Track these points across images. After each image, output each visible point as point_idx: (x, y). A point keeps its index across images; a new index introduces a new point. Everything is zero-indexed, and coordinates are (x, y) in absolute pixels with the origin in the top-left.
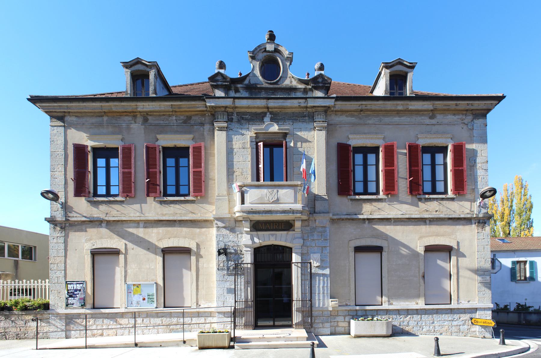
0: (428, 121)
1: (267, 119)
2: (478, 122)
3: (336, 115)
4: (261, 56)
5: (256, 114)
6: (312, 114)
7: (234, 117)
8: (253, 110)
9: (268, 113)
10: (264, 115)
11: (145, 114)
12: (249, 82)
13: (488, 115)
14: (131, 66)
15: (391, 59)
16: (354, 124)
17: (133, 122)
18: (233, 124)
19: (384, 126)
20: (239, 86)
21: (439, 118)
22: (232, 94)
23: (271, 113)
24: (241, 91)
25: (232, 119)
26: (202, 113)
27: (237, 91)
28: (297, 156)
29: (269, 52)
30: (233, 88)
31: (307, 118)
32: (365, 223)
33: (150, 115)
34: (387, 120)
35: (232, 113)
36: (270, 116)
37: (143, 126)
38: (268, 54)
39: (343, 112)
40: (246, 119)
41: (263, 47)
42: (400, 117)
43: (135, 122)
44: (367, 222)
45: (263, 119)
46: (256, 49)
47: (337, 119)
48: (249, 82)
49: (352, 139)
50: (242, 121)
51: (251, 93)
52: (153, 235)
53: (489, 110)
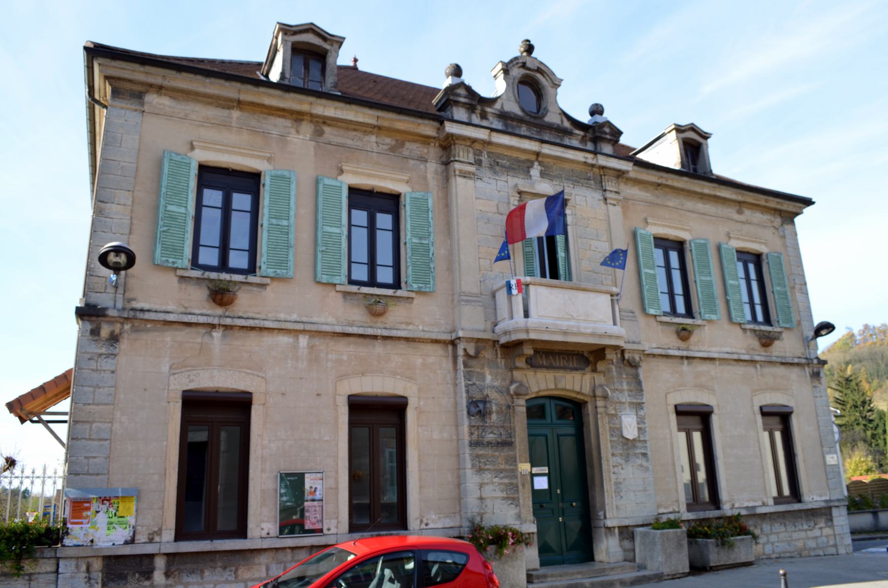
0: (736, 216)
1: (535, 172)
2: (788, 227)
3: (625, 183)
4: (517, 72)
5: (517, 160)
6: (599, 178)
7: (483, 158)
8: (515, 154)
9: (536, 164)
10: (529, 165)
11: (321, 121)
12: (502, 107)
13: (797, 220)
14: (295, 33)
15: (684, 122)
16: (651, 204)
17: (293, 131)
18: (483, 170)
19: (689, 214)
20: (489, 110)
21: (748, 213)
22: (476, 119)
23: (540, 163)
24: (491, 118)
25: (481, 161)
26: (425, 140)
27: (484, 116)
28: (584, 240)
29: (529, 69)
30: (478, 112)
31: (592, 182)
32: (683, 364)
33: (329, 125)
34: (690, 204)
35: (481, 152)
36: (539, 168)
37: (314, 143)
38: (528, 72)
39: (637, 182)
40: (503, 166)
41: (521, 61)
42: (704, 204)
43: (298, 132)
44: (686, 362)
45: (529, 172)
46: (511, 61)
47: (628, 191)
48: (502, 107)
49: (652, 224)
50: (497, 168)
51: (506, 125)
52: (329, 364)
53: (797, 214)
